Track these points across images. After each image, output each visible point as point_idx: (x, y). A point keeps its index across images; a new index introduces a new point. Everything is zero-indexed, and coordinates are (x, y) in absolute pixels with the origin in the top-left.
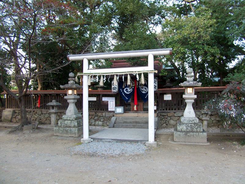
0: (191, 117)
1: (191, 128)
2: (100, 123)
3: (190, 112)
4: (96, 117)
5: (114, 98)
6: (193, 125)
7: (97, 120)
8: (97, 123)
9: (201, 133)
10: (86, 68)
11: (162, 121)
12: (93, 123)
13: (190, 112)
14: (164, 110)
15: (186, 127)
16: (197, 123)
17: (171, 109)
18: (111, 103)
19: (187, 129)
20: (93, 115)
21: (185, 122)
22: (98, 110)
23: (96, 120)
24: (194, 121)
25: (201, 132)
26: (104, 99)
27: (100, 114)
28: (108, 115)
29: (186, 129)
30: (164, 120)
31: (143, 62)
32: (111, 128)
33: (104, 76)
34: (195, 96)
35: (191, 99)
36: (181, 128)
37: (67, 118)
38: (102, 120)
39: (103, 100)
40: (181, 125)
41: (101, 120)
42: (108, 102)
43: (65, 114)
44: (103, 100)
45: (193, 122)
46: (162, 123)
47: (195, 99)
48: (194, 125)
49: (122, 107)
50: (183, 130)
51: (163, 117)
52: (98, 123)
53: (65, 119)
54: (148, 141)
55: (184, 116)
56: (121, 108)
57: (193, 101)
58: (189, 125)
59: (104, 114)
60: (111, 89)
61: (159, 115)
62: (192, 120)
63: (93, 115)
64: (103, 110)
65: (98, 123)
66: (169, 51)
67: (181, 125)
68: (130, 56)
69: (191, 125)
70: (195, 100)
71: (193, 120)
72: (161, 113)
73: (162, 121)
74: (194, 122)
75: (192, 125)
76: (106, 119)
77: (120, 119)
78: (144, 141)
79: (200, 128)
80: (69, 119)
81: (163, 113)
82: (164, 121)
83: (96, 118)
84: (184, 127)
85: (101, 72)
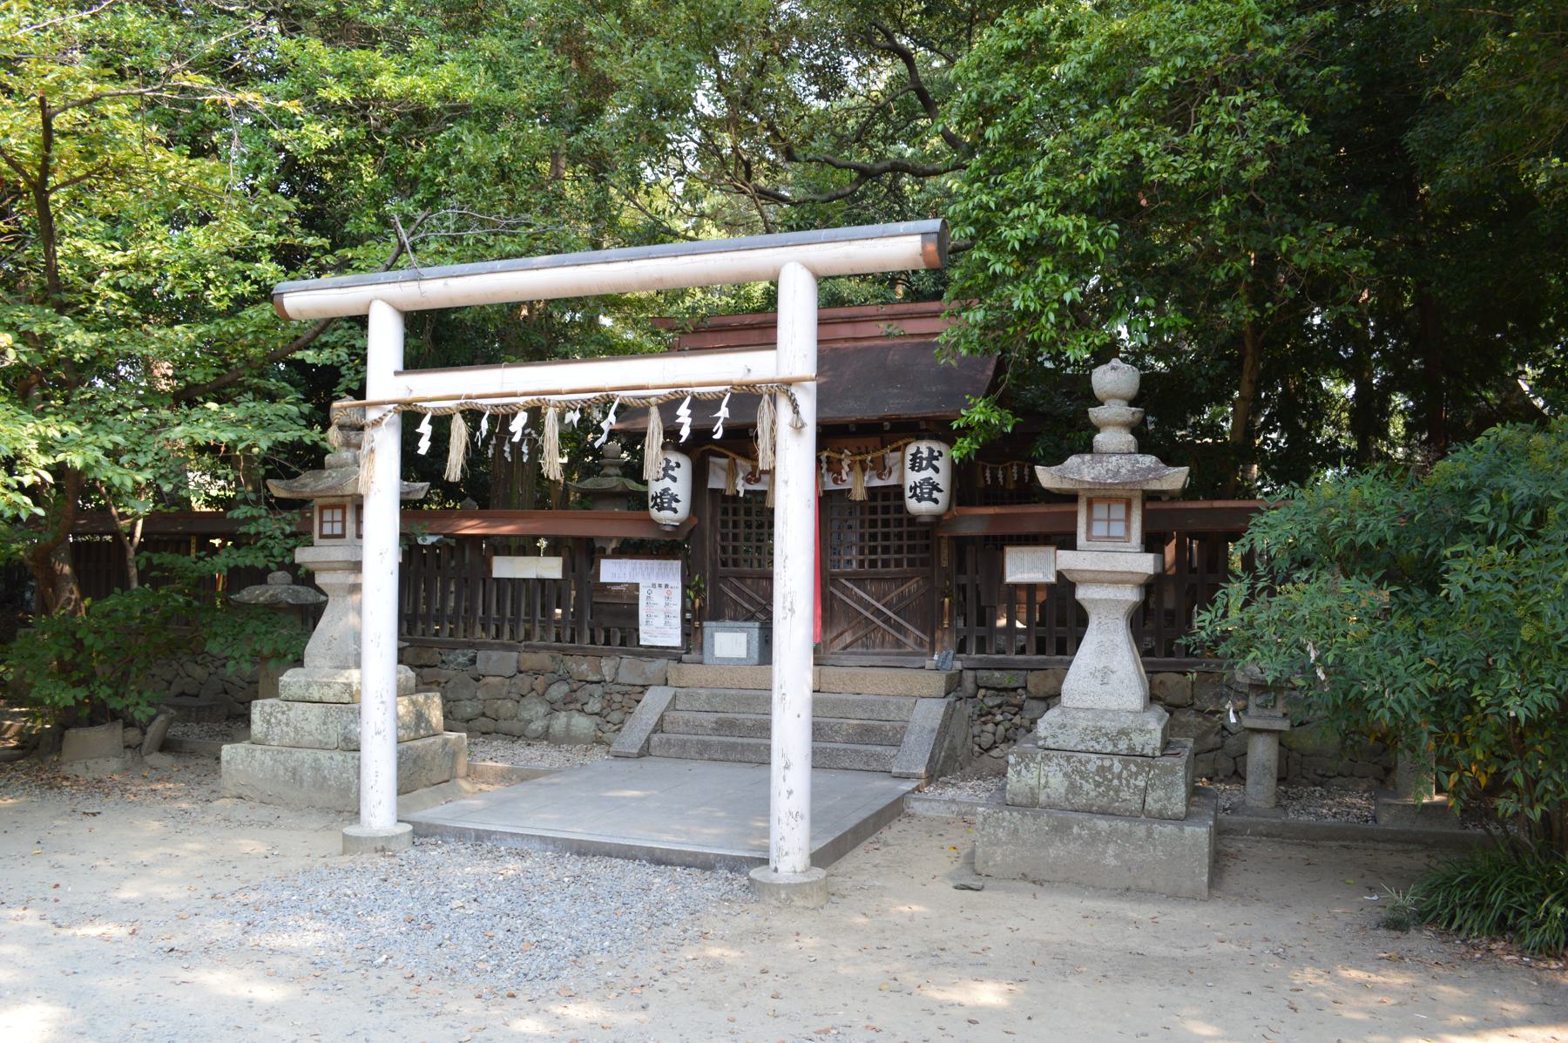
0: (1113, 705)
1: (1098, 785)
2: (582, 724)
3: (1105, 674)
4: (554, 687)
5: (676, 565)
6: (1117, 767)
7: (568, 702)
8: (560, 722)
9: (1169, 829)
10: (386, 374)
11: (990, 727)
12: (537, 726)
13: (1105, 674)
14: (1022, 651)
15: (1065, 774)
16: (1148, 751)
17: (1051, 646)
18: (658, 597)
19: (1073, 789)
20: (537, 673)
21: (1070, 740)
22: (572, 641)
23: (553, 708)
24: (1127, 735)
25: (1176, 819)
26: (612, 571)
27: (584, 667)
28: (626, 669)
29: (1063, 791)
30: (999, 718)
31: (752, 322)
32: (627, 757)
33: (472, 416)
34: (1146, 564)
35: (1116, 579)
36: (1034, 782)
37: (309, 685)
38: (594, 705)
39: (603, 579)
40: (1033, 760)
41: (588, 708)
42: (636, 586)
43: (299, 662)
44: (603, 579)
45: (1123, 746)
46: (987, 739)
47: (1142, 580)
48: (1125, 767)
49: (707, 631)
50: (1042, 798)
51: (998, 701)
52: (568, 725)
53: (295, 691)
54: (766, 862)
55: (1065, 699)
56: (741, 629)
57: (1131, 595)
58: (1092, 767)
59: (607, 667)
60: (646, 507)
61: (969, 684)
62: (1111, 726)
63: (537, 673)
64: (607, 642)
65: (568, 725)
66: (919, 238)
67: (1033, 760)
68: (661, 280)
69: (1101, 770)
70: (1151, 586)
71: (1123, 732)
72: (980, 673)
73: (990, 727)
74: (1130, 748)
75: (1107, 763)
76: (618, 698)
77: (697, 705)
78: (744, 867)
79: (1166, 787)
80: (316, 697)
81: (997, 674)
82: (1001, 727)
83: (558, 691)
84: (1051, 779)
85: (464, 391)
